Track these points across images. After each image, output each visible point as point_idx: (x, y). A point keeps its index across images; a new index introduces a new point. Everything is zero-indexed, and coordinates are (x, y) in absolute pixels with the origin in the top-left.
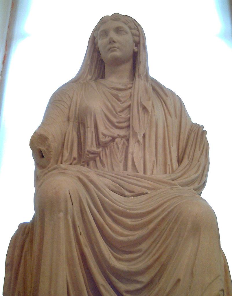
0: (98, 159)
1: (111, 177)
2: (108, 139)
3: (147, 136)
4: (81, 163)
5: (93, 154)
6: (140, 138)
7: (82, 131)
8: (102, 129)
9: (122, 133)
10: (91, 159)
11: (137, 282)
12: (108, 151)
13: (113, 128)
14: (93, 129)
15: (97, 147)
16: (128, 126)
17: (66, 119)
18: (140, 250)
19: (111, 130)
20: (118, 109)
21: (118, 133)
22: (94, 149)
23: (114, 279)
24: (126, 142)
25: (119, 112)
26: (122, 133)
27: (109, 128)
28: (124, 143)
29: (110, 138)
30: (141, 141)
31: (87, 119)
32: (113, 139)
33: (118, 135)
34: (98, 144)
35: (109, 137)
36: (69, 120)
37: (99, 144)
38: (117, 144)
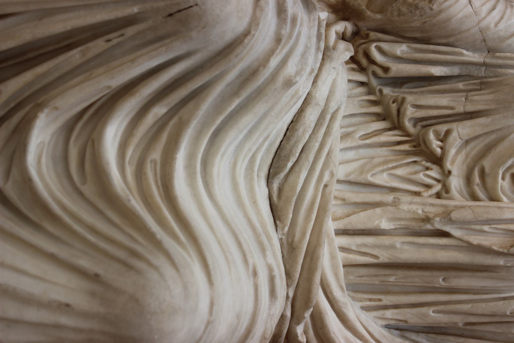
1: (317, 145)
2: (435, 144)
4: (379, 87)
5: (399, 111)
6: (438, 225)
7: (460, 86)
10: (387, 109)
12: (406, 147)
13: (468, 160)
14: (460, 109)
15: (416, 121)
17: (490, 44)
18: (84, 181)
19: (460, 158)
21: (455, 171)
22: (410, 112)
24: (434, 191)
27: (468, 148)
28: (428, 187)
29: (439, 151)
30: (429, 227)
31: (489, 94)
33: (450, 172)
34: (425, 123)
35: (441, 148)
36: (490, 51)
38: (427, 169)
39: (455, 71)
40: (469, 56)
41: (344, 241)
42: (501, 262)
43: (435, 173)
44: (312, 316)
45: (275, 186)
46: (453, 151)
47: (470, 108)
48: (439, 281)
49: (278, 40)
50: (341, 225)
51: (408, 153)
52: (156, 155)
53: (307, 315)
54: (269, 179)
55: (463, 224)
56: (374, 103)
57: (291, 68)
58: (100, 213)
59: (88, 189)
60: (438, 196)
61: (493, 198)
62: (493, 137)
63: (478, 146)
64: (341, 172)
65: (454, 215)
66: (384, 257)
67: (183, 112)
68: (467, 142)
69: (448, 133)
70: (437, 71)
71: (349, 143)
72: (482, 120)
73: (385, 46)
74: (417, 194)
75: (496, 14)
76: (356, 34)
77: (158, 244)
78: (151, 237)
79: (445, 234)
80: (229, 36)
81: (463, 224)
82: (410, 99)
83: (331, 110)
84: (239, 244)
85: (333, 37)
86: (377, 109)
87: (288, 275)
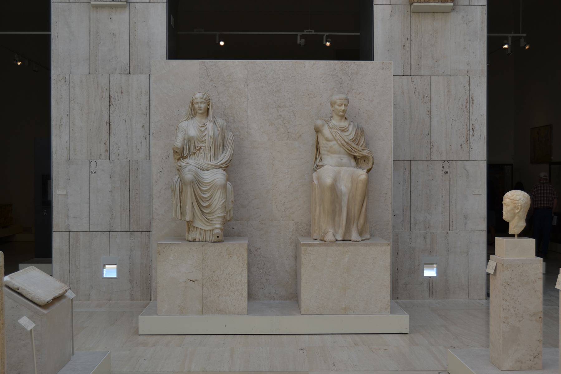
0: (195, 154)
2: (198, 148)
3: (211, 147)
7: (190, 143)
8: (197, 145)
9: (203, 145)
11: (207, 199)
12: (199, 152)
14: (194, 144)
15: (195, 150)
16: (206, 142)
19: (200, 144)
20: (202, 137)
21: (202, 145)
22: (194, 151)
23: (202, 198)
25: (203, 137)
26: (203, 145)
32: (201, 147)
37: (195, 148)
39: (187, 144)
40: (186, 142)
41: (212, 161)
42: (214, 140)
43: (202, 148)
44: (221, 165)
45: (206, 170)
46: (200, 146)
47: (193, 143)
48: (216, 147)
49: (192, 171)
50: (210, 161)
51: (199, 151)
52: (205, 184)
53: (221, 165)
54: (205, 171)
55: (209, 145)
56: (192, 155)
57: (194, 170)
58: (211, 190)
59: (209, 191)
60: (205, 147)
61: (206, 140)
62: (198, 141)
63: (198, 142)
64: (203, 161)
65: (208, 146)
66: (214, 155)
67: (200, 181)
68: (198, 143)
69: (197, 146)
70: (188, 147)
71: (199, 160)
72: (195, 142)
73: (184, 154)
74: (205, 150)
75: (180, 139)
76: (182, 157)
77: (215, 184)
78: (214, 185)
79: (211, 147)
80: (193, 177)
81: (209, 145)
82: (192, 151)
83: (195, 163)
84: (213, 175)
85: (184, 162)
86: (193, 155)
87: (216, 168)
